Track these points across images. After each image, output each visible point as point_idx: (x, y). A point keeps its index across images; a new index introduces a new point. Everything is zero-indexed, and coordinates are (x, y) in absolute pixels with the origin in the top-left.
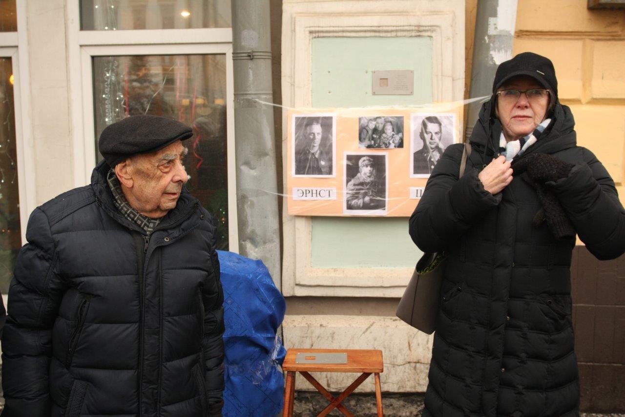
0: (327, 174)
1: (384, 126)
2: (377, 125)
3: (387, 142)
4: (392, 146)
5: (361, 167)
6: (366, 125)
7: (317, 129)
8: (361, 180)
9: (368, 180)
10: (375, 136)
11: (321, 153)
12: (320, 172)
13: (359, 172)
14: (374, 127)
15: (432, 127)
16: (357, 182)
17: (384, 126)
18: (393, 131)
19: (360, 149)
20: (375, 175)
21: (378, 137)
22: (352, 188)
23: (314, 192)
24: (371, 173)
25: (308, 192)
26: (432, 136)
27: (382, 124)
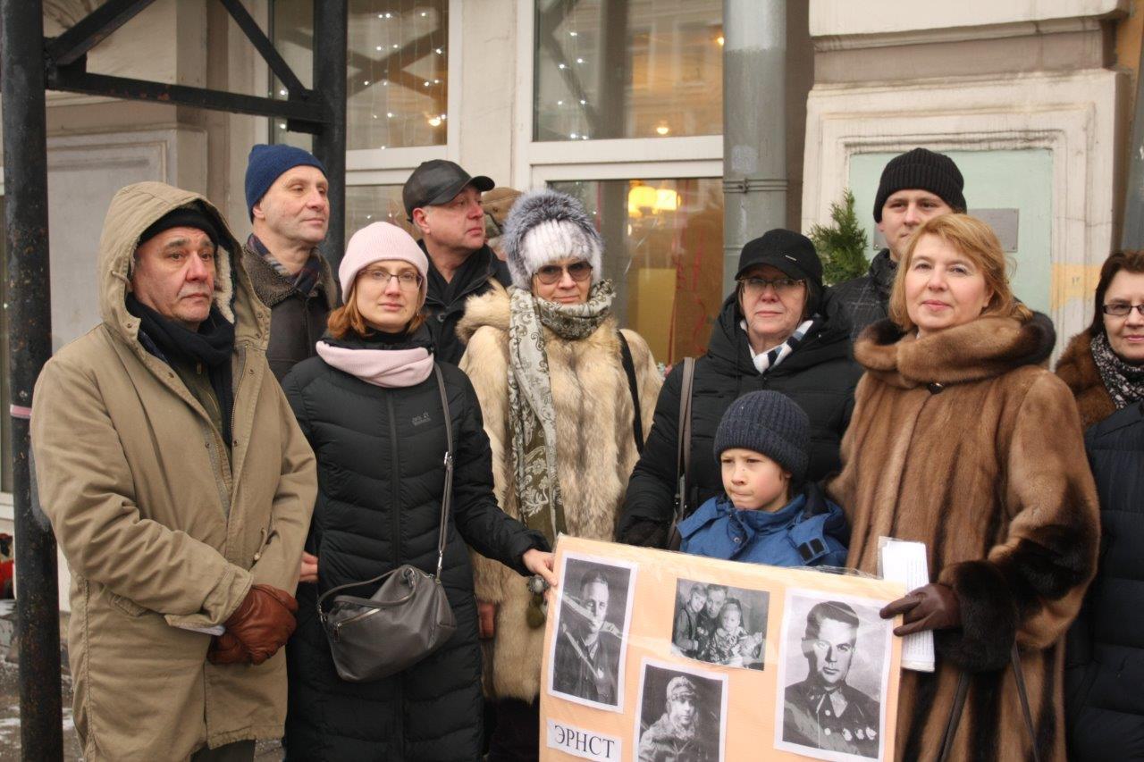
0: (606, 703)
1: (723, 610)
2: (709, 605)
3: (725, 650)
4: (737, 661)
5: (669, 701)
6: (687, 601)
7: (600, 591)
8: (669, 733)
9: (683, 735)
10: (701, 631)
11: (600, 650)
12: (594, 697)
13: (666, 712)
14: (701, 607)
15: (834, 631)
16: (661, 734)
17: (723, 610)
18: (742, 625)
19: (671, 658)
20: (697, 725)
21: (707, 633)
22: (648, 745)
23: (581, 738)
24: (690, 718)
25: (571, 736)
26: (830, 652)
27: (718, 603)
